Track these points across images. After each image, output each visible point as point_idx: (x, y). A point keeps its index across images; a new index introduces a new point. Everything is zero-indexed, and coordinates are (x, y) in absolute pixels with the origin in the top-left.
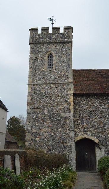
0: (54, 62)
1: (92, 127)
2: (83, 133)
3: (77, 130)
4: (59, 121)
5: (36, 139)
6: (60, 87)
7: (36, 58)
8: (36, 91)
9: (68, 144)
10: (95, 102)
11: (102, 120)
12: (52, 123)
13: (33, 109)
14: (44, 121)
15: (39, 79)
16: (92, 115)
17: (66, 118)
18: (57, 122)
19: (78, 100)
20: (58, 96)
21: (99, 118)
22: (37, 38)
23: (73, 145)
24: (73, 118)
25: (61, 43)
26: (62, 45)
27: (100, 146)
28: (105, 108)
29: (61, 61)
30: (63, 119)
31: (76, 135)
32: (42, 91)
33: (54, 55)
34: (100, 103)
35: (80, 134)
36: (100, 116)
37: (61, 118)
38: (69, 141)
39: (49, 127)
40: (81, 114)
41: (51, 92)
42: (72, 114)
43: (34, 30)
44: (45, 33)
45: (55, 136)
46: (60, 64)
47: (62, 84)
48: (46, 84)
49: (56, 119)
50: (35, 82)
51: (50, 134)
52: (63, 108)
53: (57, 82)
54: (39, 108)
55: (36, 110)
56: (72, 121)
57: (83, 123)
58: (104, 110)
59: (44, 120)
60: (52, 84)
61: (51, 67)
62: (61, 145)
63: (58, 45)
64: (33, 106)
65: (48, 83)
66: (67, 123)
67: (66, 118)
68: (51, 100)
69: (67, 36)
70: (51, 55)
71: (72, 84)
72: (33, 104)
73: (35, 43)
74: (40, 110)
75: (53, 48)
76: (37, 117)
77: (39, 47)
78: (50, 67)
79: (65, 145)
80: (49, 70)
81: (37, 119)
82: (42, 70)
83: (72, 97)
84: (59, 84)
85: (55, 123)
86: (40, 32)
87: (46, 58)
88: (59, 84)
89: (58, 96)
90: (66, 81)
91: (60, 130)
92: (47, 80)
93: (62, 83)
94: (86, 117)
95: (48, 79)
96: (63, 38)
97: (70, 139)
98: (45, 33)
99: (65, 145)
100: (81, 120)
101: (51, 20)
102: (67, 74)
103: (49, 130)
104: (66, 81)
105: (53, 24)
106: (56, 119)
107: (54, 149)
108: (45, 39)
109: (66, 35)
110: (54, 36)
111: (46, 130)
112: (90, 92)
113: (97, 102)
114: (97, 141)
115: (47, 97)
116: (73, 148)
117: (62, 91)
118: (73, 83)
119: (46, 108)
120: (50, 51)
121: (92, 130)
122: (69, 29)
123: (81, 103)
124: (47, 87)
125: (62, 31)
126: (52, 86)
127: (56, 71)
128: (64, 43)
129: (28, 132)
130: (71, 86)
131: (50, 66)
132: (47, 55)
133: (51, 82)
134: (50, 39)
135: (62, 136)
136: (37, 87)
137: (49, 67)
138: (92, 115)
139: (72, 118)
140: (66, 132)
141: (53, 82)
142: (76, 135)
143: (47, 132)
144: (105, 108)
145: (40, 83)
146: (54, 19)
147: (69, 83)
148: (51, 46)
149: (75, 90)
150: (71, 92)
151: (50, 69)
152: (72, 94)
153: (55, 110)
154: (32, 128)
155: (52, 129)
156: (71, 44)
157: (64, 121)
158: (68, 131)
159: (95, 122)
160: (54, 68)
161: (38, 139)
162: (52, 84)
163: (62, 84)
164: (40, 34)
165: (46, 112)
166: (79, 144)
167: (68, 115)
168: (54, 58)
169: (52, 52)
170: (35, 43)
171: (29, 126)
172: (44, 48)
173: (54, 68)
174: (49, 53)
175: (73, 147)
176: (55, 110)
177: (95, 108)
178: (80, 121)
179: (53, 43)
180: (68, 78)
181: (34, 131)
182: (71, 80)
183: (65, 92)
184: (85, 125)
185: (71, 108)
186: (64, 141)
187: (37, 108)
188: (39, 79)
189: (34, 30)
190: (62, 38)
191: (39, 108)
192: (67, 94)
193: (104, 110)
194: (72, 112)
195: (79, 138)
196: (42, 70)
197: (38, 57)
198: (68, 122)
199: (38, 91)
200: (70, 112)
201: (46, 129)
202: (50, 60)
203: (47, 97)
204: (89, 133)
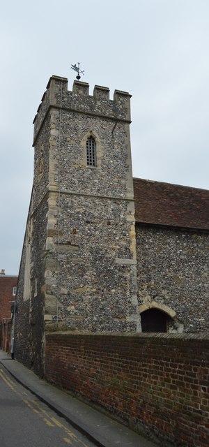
0: (99, 154)
1: (163, 288)
2: (149, 298)
4: (110, 273)
5: (69, 309)
6: (112, 207)
8: (66, 207)
9: (129, 319)
10: (169, 241)
13: (61, 244)
14: (84, 271)
15: (71, 183)
16: (164, 265)
17: (123, 267)
18: (109, 275)
19: (142, 235)
20: (109, 224)
21: (175, 271)
22: (65, 99)
25: (112, 119)
27: (177, 324)
28: (184, 255)
29: (112, 154)
30: (119, 270)
31: (140, 302)
32: (77, 210)
33: (98, 140)
34: (177, 244)
38: (131, 313)
40: (145, 261)
42: (134, 261)
43: (57, 81)
44: (81, 92)
45: (105, 302)
47: (115, 200)
49: (106, 268)
50: (64, 189)
51: (96, 299)
52: (118, 247)
53: (105, 195)
54: (73, 243)
55: (66, 247)
56: (135, 274)
57: (149, 280)
58: (182, 257)
59: (83, 270)
60: (98, 197)
61: (91, 164)
64: (60, 239)
66: (125, 278)
67: (124, 268)
69: (121, 110)
70: (92, 139)
71: (133, 203)
73: (63, 109)
75: (97, 127)
77: (70, 118)
78: (89, 162)
79: (123, 321)
83: (133, 228)
84: (110, 199)
85: (105, 276)
86: (70, 87)
87: (84, 143)
88: (110, 199)
89: (109, 224)
90: (122, 195)
91: (113, 290)
92: (86, 187)
94: (154, 268)
95: (89, 186)
96: (112, 111)
98: (81, 92)
99: (123, 321)
100: (145, 273)
101: (76, 69)
102: (123, 181)
103: (94, 290)
104: (122, 195)
105: (78, 77)
106: (106, 268)
107: (103, 329)
108: (82, 106)
109: (121, 106)
110: (99, 103)
111: (88, 290)
112: (160, 222)
113: (172, 241)
114: (172, 313)
115: (88, 222)
116: (138, 327)
117: (116, 213)
120: (91, 132)
121: (164, 292)
122: (123, 96)
124: (88, 202)
126: (97, 201)
127: (104, 173)
128: (116, 120)
129: (52, 293)
130: (131, 207)
131: (92, 161)
132: (85, 138)
133: (95, 193)
134: (92, 108)
135: (117, 302)
136: (68, 200)
137: (88, 163)
138: (164, 265)
139: (134, 269)
140: (125, 295)
141: (99, 195)
142: (140, 302)
143: (91, 295)
144: (184, 255)
145: (73, 192)
146: (81, 69)
147: (128, 201)
148: (93, 121)
150: (131, 219)
152: (134, 223)
153: (104, 251)
154: (59, 284)
155: (99, 289)
158: (128, 293)
159: (168, 279)
160: (99, 167)
161: (73, 307)
162: (98, 197)
163: (115, 200)
164: (71, 93)
165: (87, 254)
166: (144, 315)
168: (99, 147)
171: (53, 279)
172: (80, 122)
173: (99, 167)
174: (89, 134)
175: (138, 324)
178: (145, 276)
179: (97, 116)
180: (126, 191)
181: (65, 290)
182: (131, 195)
183: (122, 216)
184: (153, 283)
185: (133, 248)
186: (121, 314)
187: (69, 243)
188: (71, 183)
191: (73, 243)
192: (125, 221)
194: (135, 257)
195: (145, 307)
197: (69, 139)
198: (128, 275)
199: (71, 208)
200: (130, 257)
201: (88, 289)
202: (89, 149)
203: (88, 222)
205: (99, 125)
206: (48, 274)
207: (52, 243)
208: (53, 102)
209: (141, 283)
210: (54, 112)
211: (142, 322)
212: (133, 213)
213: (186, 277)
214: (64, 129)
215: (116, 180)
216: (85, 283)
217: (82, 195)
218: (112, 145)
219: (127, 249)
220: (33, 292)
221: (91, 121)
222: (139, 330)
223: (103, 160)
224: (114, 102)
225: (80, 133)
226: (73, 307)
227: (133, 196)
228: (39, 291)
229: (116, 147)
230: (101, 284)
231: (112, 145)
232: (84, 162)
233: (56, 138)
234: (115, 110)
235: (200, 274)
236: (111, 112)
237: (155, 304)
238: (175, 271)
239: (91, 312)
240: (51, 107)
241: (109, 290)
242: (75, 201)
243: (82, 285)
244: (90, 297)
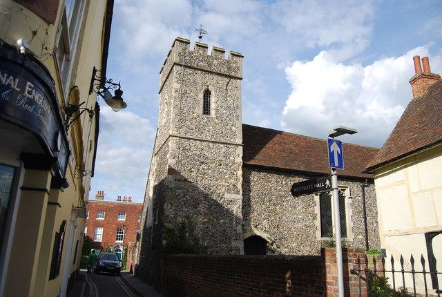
0: (213, 106)
6: (223, 149)
9: (234, 244)
13: (179, 180)
14: (198, 204)
17: (231, 201)
22: (187, 58)
23: (241, 245)
26: (227, 80)
31: (244, 230)
32: (194, 152)
33: (213, 93)
41: (210, 156)
46: (225, 112)
48: (201, 141)
50: (183, 135)
60: (212, 142)
62: (223, 245)
63: (220, 78)
70: (207, 93)
75: (213, 82)
81: (184, 199)
84: (222, 143)
87: (201, 96)
88: (222, 143)
91: (222, 221)
93: (226, 144)
97: (237, 237)
98: (201, 52)
103: (206, 220)
104: (232, 140)
105: (200, 37)
110: (215, 62)
115: (203, 163)
125: (227, 56)
126: (211, 145)
129: (170, 222)
130: (241, 148)
131: (206, 110)
133: (209, 139)
134: (210, 65)
139: (240, 202)
145: (191, 137)
162: (212, 142)
167: (234, 196)
168: (213, 99)
169: (210, 88)
170: (185, 66)
172: (199, 77)
176: (215, 187)
181: (180, 219)
182: (239, 140)
183: (231, 158)
186: (227, 239)
190: (228, 68)
194: (241, 192)
200: (238, 192)
203: (203, 163)
205: (215, 81)
206: (167, 206)
207: (171, 179)
208: (177, 60)
210: (176, 68)
211: (245, 248)
212: (241, 155)
214: (182, 81)
216: (199, 213)
218: (225, 97)
220: (154, 220)
221: (209, 76)
222: (242, 253)
223: (217, 111)
224: (228, 62)
227: (242, 141)
228: (159, 221)
231: (225, 97)
232: (200, 111)
234: (229, 69)
235: (295, 207)
236: (226, 70)
239: (203, 238)
240: (175, 64)
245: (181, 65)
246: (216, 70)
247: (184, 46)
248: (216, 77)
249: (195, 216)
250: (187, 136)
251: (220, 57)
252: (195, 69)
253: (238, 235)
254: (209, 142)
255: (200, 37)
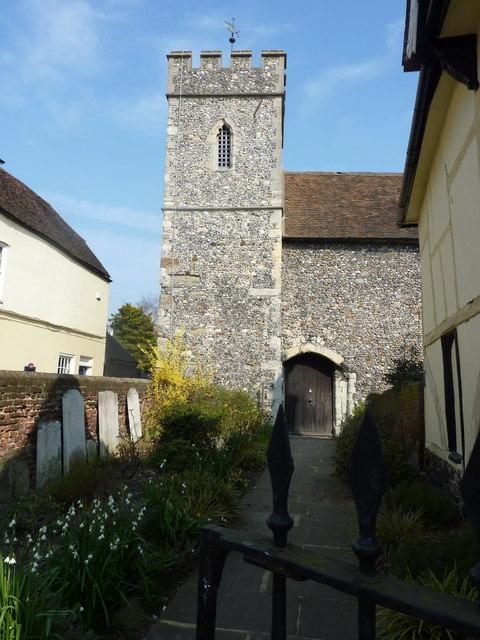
0: (235, 150)
1: (326, 326)
3: (288, 332)
6: (247, 218)
7: (186, 137)
8: (185, 228)
9: (265, 366)
11: (354, 307)
12: (226, 312)
13: (177, 275)
17: (260, 300)
18: (238, 309)
19: (295, 253)
21: (346, 301)
22: (188, 82)
23: (277, 369)
24: (279, 301)
25: (255, 96)
26: (255, 103)
28: (364, 277)
29: (252, 146)
32: (200, 230)
33: (234, 129)
34: (352, 263)
35: (296, 342)
36: (348, 296)
37: (250, 301)
38: (267, 359)
39: (218, 322)
41: (225, 232)
42: (277, 290)
44: (210, 66)
48: (212, 210)
50: (182, 205)
52: (254, 274)
54: (192, 272)
56: (278, 308)
57: (304, 314)
58: (360, 281)
60: (228, 210)
64: (175, 269)
65: (216, 206)
66: (262, 315)
68: (223, 253)
70: (226, 129)
72: (177, 262)
73: (184, 96)
74: (194, 278)
75: (231, 110)
76: (186, 298)
80: (221, 172)
82: (201, 171)
83: (279, 245)
87: (213, 139)
88: (246, 210)
89: (243, 244)
90: (263, 202)
91: (245, 331)
93: (251, 209)
94: (312, 298)
98: (210, 66)
102: (266, 183)
103: (220, 330)
104: (263, 202)
108: (211, 85)
109: (269, 74)
110: (235, 76)
112: (324, 234)
113: (344, 258)
114: (337, 359)
115: (213, 244)
117: (253, 228)
118: (282, 209)
119: (211, 275)
121: (325, 331)
123: (300, 262)
124: (214, 217)
126: (227, 215)
127: (238, 175)
130: (278, 218)
133: (224, 205)
134: (225, 85)
136: (187, 218)
138: (329, 294)
139: (277, 302)
142: (287, 345)
144: (364, 277)
147: (272, 209)
148: (227, 102)
149: (288, 227)
150: (278, 233)
151: (225, 168)
152: (280, 240)
153: (233, 280)
154: (174, 324)
156: (280, 99)
157: (256, 308)
158: (265, 334)
160: (234, 168)
161: (189, 353)
162: (228, 210)
165: (210, 285)
166: (289, 365)
167: (265, 292)
168: (235, 140)
169: (228, 121)
170: (184, 96)
172: (207, 109)
174: (221, 124)
177: (338, 277)
178: (298, 310)
182: (277, 202)
183: (262, 232)
185: (276, 273)
186: (253, 360)
187: (188, 274)
189: (180, 57)
191: (192, 272)
192: (266, 238)
193: (360, 281)
194: (279, 285)
195: (292, 353)
196: (201, 171)
198: (265, 310)
200: (272, 285)
201: (211, 329)
203: (213, 244)
204: (319, 339)
209: (287, 322)
212: (279, 226)
213: (365, 309)
215: (256, 181)
217: (207, 210)
219: (267, 275)
225: (208, 122)
226: (189, 353)
229: (259, 134)
230: (228, 322)
231: (252, 134)
233: (174, 138)
234: (260, 81)
237: (310, 348)
238: (346, 301)
241: (239, 330)
242: (198, 217)
243: (202, 325)
244: (212, 339)
245: (178, 96)
246: (236, 90)
247: (179, 65)
248: (233, 103)
249: (202, 325)
250: (190, 207)
251: (242, 66)
252: (199, 96)
253: (272, 352)
254: (224, 210)
255: (232, 41)
